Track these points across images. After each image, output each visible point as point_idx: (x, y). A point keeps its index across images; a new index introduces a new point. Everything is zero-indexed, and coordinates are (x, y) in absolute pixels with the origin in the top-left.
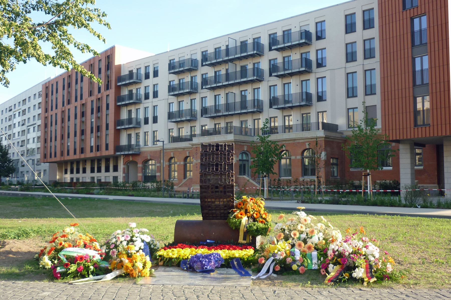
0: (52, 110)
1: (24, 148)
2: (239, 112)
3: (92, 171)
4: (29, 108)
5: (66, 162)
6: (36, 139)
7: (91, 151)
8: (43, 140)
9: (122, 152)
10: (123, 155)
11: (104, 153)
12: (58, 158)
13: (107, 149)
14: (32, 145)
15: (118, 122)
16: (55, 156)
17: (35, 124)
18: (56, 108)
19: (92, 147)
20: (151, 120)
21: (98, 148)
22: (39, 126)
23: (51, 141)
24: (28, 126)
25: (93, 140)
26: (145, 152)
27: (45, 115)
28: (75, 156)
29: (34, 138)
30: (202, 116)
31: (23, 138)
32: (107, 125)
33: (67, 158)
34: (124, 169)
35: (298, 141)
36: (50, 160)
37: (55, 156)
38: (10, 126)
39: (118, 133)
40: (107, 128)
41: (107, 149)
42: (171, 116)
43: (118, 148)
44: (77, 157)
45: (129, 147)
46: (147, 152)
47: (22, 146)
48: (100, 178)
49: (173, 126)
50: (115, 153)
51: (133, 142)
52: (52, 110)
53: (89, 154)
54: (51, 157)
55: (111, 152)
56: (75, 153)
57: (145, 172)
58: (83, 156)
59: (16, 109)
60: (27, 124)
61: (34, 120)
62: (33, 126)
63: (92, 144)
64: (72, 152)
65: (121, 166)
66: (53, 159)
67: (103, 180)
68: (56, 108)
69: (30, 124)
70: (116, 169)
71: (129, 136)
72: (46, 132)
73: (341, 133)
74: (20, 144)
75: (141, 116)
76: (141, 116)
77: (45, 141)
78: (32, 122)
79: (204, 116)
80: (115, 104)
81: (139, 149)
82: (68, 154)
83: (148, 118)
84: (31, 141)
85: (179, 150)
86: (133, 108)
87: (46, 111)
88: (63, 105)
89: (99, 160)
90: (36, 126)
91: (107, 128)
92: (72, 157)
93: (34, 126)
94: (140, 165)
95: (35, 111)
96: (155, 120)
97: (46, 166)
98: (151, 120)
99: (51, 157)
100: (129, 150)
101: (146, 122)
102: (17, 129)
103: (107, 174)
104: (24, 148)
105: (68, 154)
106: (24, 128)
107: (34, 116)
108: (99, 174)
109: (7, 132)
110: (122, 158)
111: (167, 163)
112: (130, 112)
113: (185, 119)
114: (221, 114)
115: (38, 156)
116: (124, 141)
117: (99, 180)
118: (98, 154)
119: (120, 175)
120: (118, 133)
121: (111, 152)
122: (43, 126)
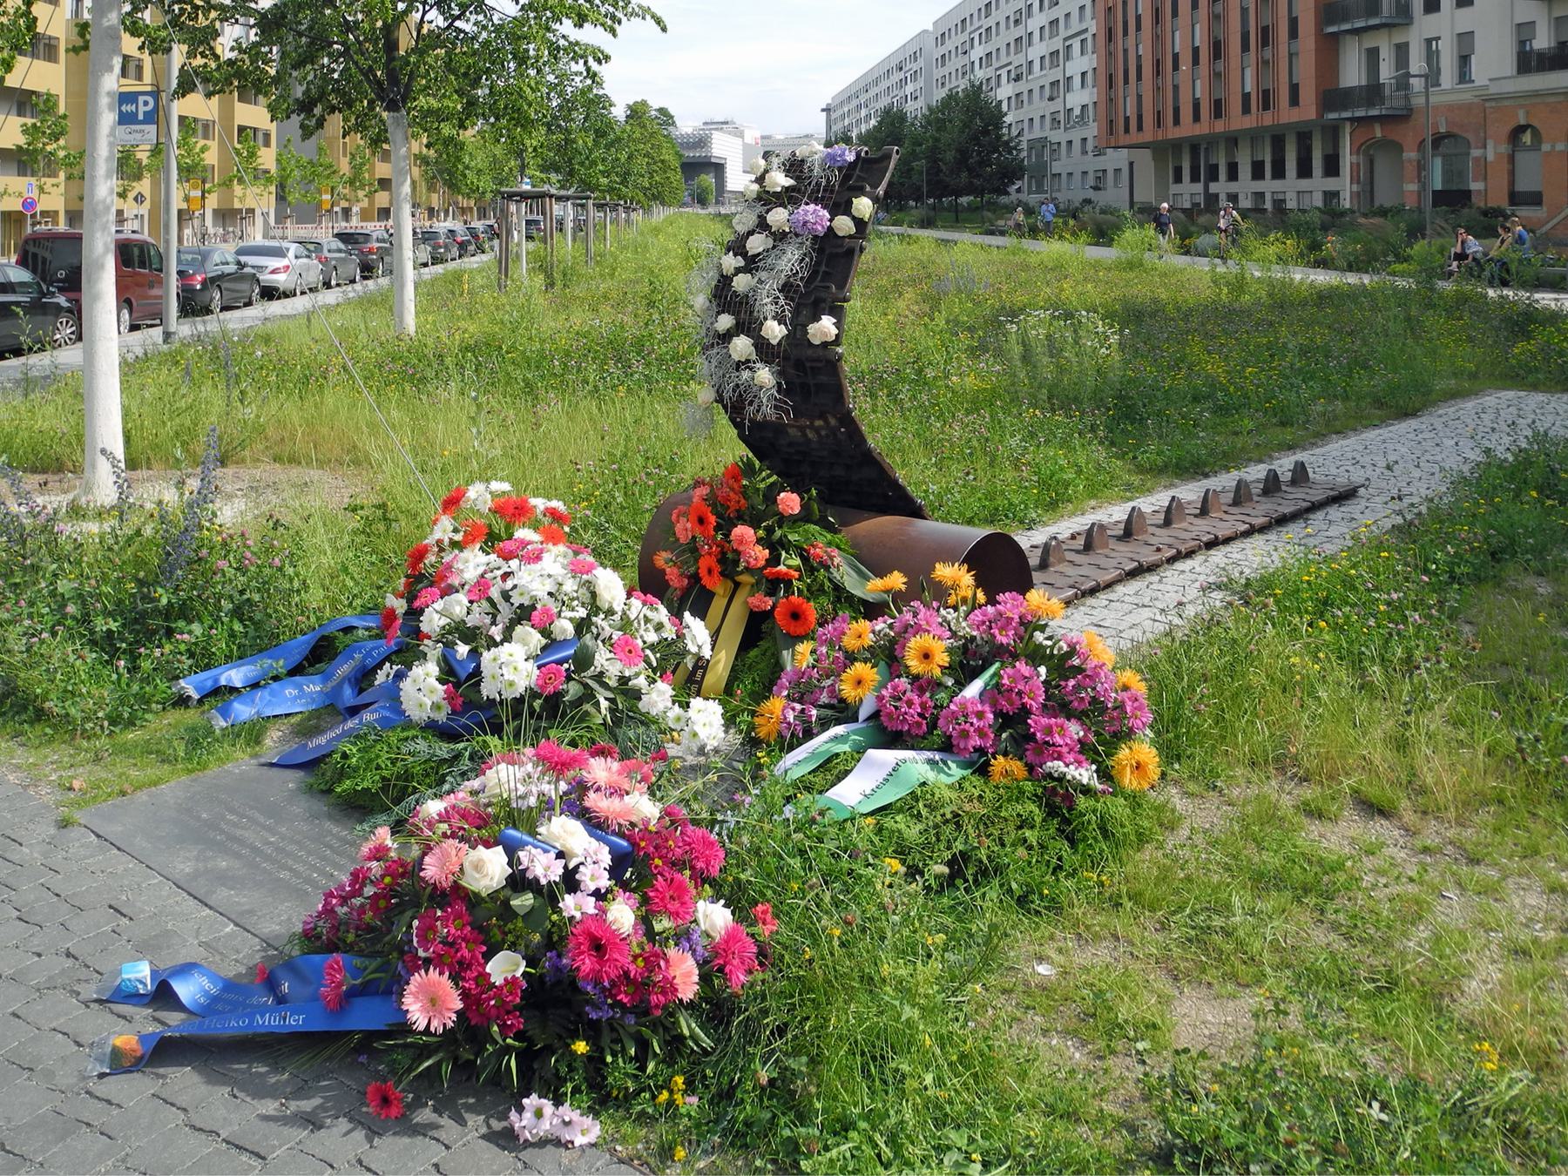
1: (1057, 105)
3: (1258, 173)
5: (1176, 146)
7: (1246, 109)
8: (1103, 79)
9: (1345, 108)
10: (1352, 120)
11: (1286, 115)
12: (1148, 135)
13: (1294, 100)
16: (1140, 128)
19: (1246, 97)
21: (1267, 100)
23: (1126, 81)
25: (1249, 74)
28: (1197, 125)
32: (1293, 24)
33: (1174, 133)
36: (1128, 140)
37: (1140, 128)
39: (1329, 47)
40: (1293, 33)
41: (1294, 100)
43: (1333, 97)
44: (1202, 129)
45: (1373, 91)
47: (1051, 99)
50: (1320, 115)
51: (1386, 72)
53: (1237, 121)
54: (1127, 130)
55: (1308, 111)
56: (1197, 117)
58: (1220, 127)
63: (1248, 90)
66: (1135, 137)
67: (1291, 204)
70: (1332, 168)
71: (1373, 55)
77: (1111, 79)
81: (1407, 97)
82: (1177, 122)
85: (1552, 99)
91: (1293, 33)
92: (1187, 129)
94: (1411, 155)
99: (1127, 130)
100: (1370, 104)
103: (1304, 184)
104: (1057, 105)
105: (1177, 122)
110: (1348, 130)
111: (1504, 148)
115: (1092, 130)
116: (1352, 74)
117: (1279, 204)
118: (1268, 119)
119: (1345, 185)
121: (1308, 111)
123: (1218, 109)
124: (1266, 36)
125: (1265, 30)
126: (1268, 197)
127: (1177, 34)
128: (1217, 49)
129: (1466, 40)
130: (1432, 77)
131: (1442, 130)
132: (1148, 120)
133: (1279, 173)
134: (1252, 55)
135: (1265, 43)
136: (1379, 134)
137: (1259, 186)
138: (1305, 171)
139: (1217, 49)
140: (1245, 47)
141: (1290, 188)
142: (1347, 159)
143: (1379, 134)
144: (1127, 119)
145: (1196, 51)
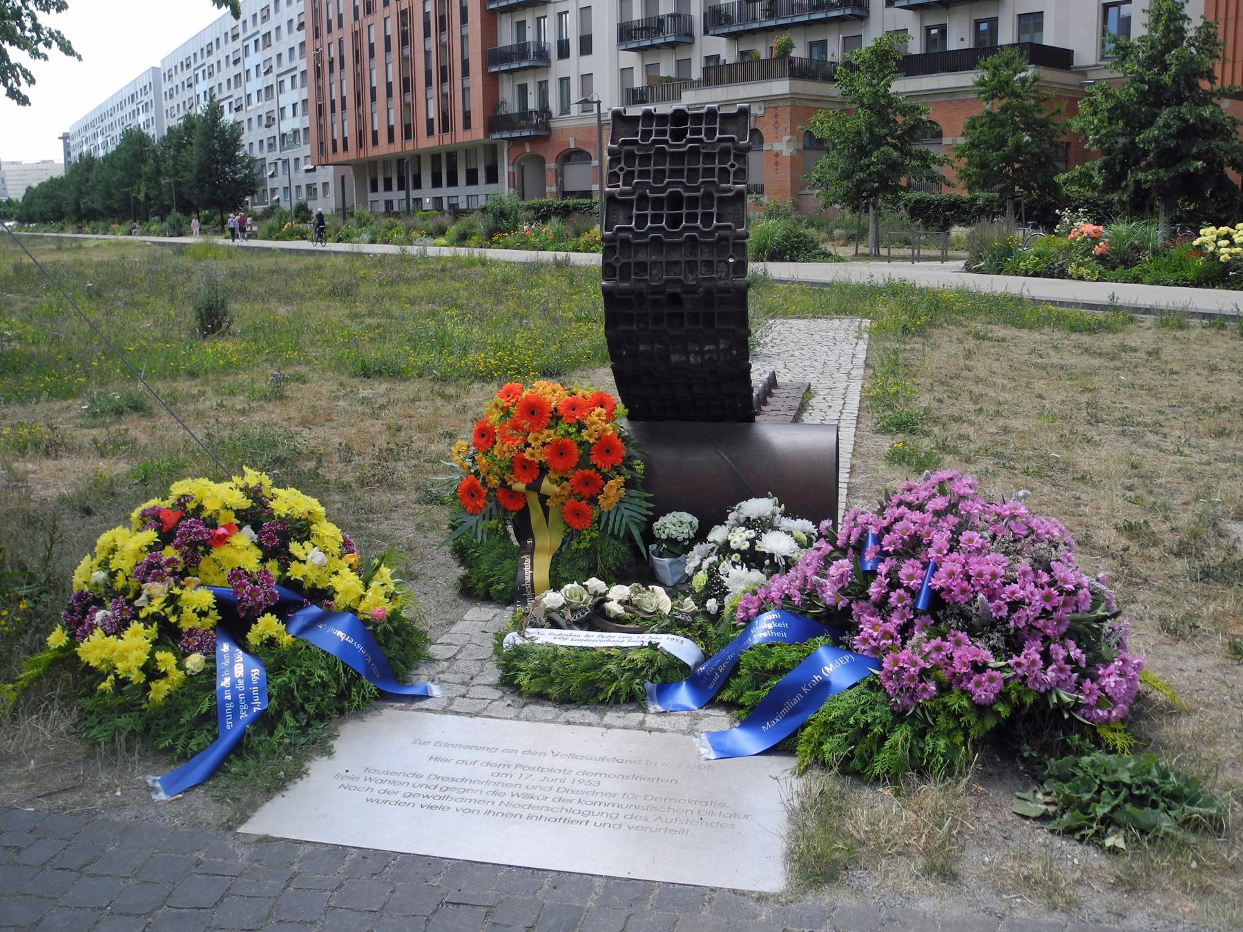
0: (330, 31)
1: (274, 131)
2: (805, 18)
3: (436, 183)
4: (278, 28)
5: (372, 164)
6: (299, 107)
7: (430, 132)
11: (462, 136)
12: (352, 154)
13: (467, 125)
14: (289, 124)
15: (493, 55)
16: (345, 148)
17: (295, 68)
18: (340, 25)
19: (430, 122)
20: (574, 47)
22: (304, 73)
23: (333, 110)
24: (278, 76)
25: (433, 105)
26: (562, 130)
27: (314, 44)
29: (294, 105)
30: (706, 32)
31: (271, 105)
33: (372, 152)
34: (511, 176)
35: (961, 97)
36: (332, 158)
37: (345, 148)
38: (237, 76)
40: (466, 72)
41: (467, 125)
42: (626, 33)
43: (495, 121)
44: (397, 148)
46: (568, 129)
48: (454, 201)
49: (631, 59)
50: (487, 135)
51: (532, 104)
52: (330, 31)
53: (424, 142)
54: (335, 150)
55: (478, 132)
56: (391, 139)
57: (562, 182)
59: (249, 34)
60: (276, 71)
61: (291, 58)
62: (290, 75)
63: (431, 116)
64: (383, 137)
65: (505, 170)
66: (341, 156)
68: (340, 25)
69: (282, 70)
71: (523, 89)
72: (319, 90)
73: (1083, 71)
74: (264, 121)
75: (550, 39)
76: (550, 39)
77: (320, 109)
78: (286, 65)
79: (711, 32)
80: (483, 6)
82: (375, 142)
83: (567, 41)
84: (289, 112)
86: (529, 17)
87: (317, 34)
88: (356, 17)
89: (452, 156)
90: (298, 72)
91: (466, 72)
93: (293, 74)
94: (551, 165)
95: (292, 35)
96: (586, 46)
97: (327, 174)
98: (574, 47)
99: (335, 150)
101: (564, 52)
102: (255, 85)
103: (472, 189)
104: (274, 131)
105: (375, 142)
106: (272, 79)
107: (292, 49)
108: (452, 191)
109: (233, 91)
112: (521, 25)
113: (662, 41)
114: (756, 25)
115: (304, 150)
120: (491, 82)
122: (311, 75)
123: (408, 132)
124: (444, 75)
125: (442, 19)
126: (445, 200)
127: (374, 72)
128: (407, 85)
129: (586, 78)
130: (565, 110)
131: (572, 146)
132: (352, 143)
133: (453, 182)
134: (434, 91)
135: (442, 29)
136: (528, 150)
137: (438, 192)
138: (472, 179)
139: (407, 85)
140: (428, 83)
141: (461, 193)
142: (505, 170)
143: (528, 150)
144: (334, 142)
145: (389, 86)
